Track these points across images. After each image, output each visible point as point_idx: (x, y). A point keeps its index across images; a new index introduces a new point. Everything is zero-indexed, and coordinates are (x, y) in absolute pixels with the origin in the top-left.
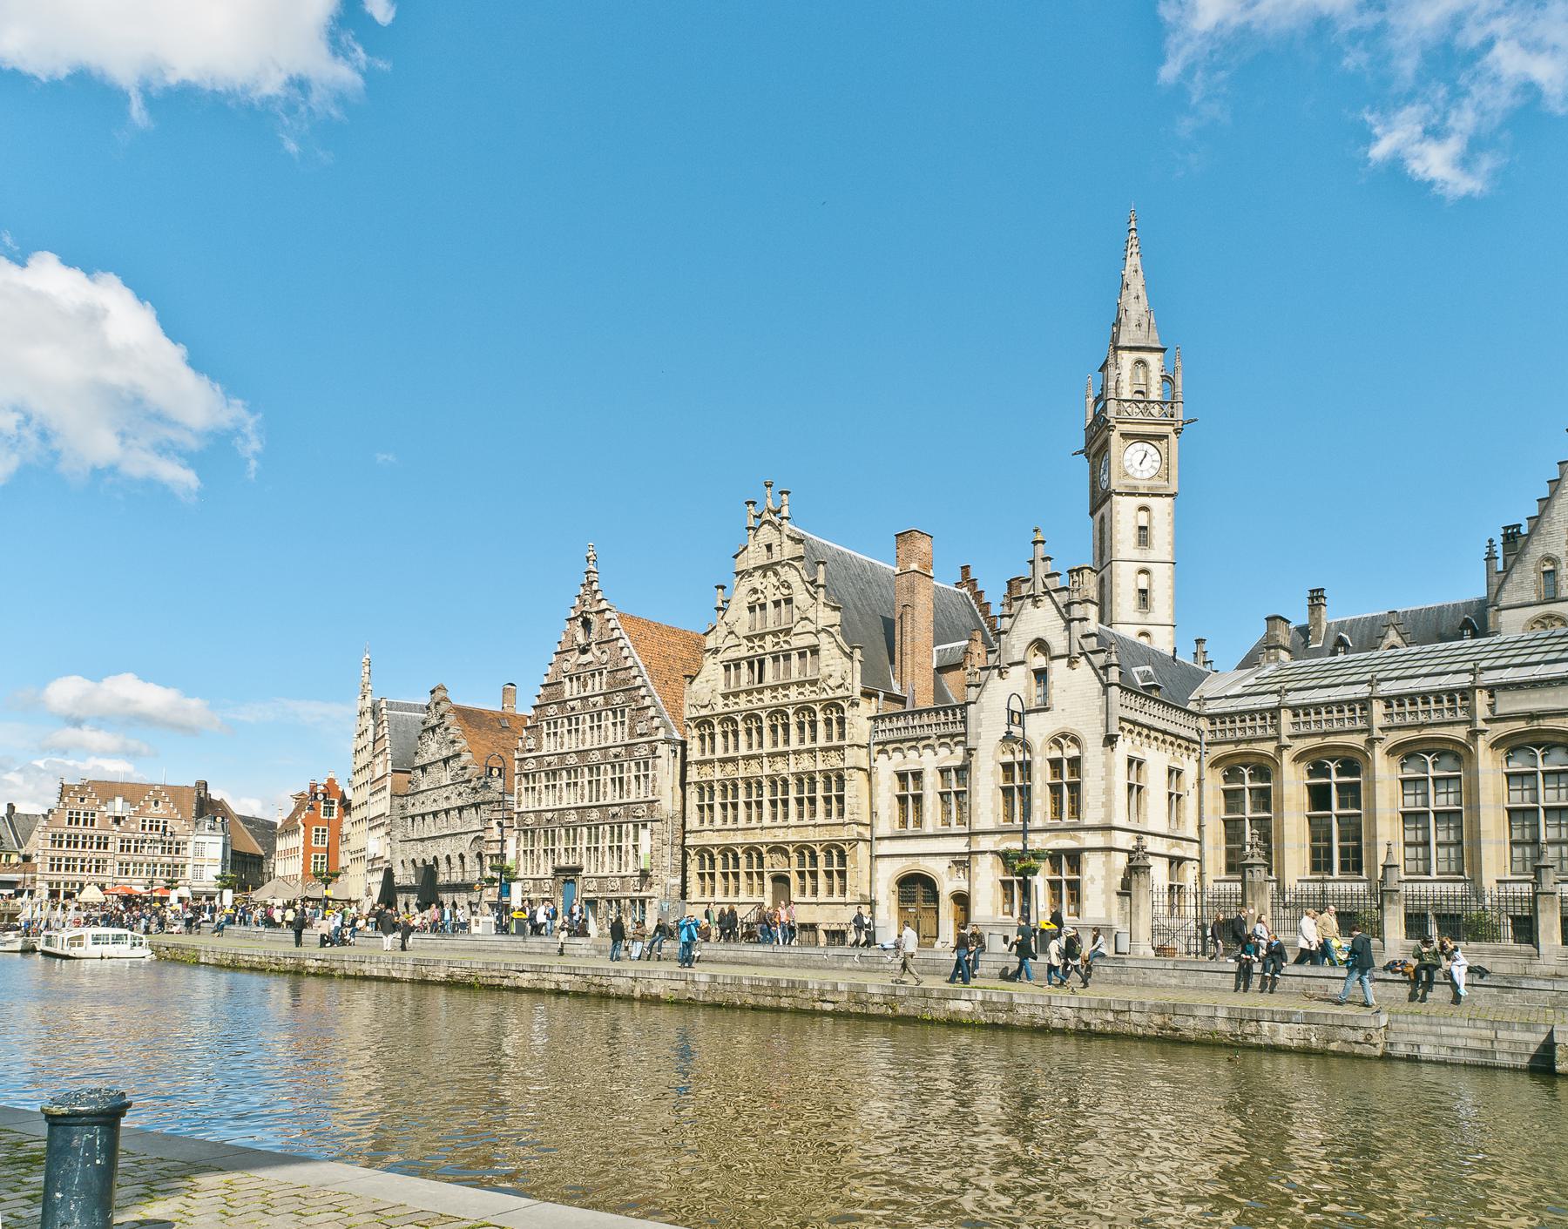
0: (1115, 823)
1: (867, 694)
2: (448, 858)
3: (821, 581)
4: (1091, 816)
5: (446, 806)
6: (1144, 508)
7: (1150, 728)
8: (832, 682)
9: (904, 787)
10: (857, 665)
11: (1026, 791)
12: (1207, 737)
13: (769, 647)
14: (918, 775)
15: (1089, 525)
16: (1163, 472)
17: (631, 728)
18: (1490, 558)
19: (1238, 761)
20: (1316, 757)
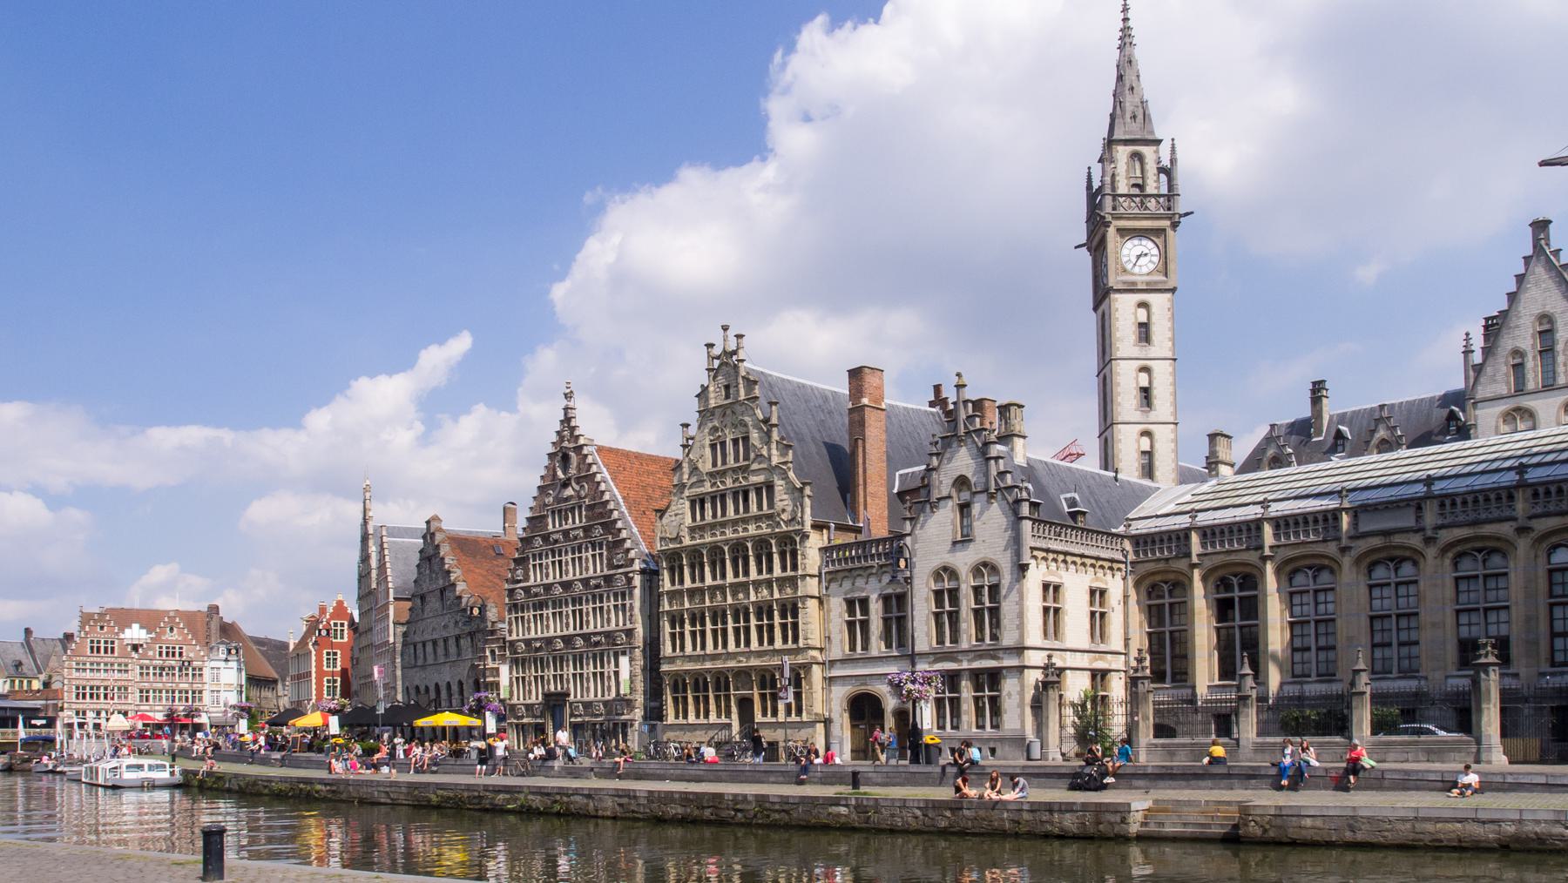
0: (1028, 643)
1: (818, 527)
2: (449, 685)
3: (774, 420)
4: (1008, 639)
5: (446, 635)
6: (1143, 305)
7: (1066, 554)
8: (785, 517)
9: (851, 612)
10: (807, 502)
11: (954, 617)
12: (1131, 557)
13: (729, 483)
14: (864, 603)
15: (1093, 318)
16: (1161, 267)
17: (610, 560)
18: (1467, 352)
19: (1158, 578)
20: (1221, 573)
